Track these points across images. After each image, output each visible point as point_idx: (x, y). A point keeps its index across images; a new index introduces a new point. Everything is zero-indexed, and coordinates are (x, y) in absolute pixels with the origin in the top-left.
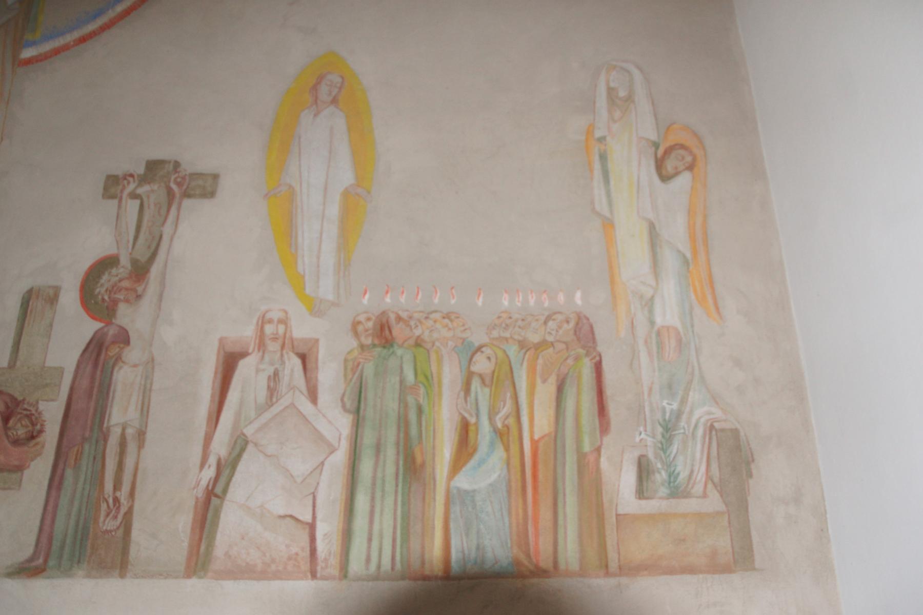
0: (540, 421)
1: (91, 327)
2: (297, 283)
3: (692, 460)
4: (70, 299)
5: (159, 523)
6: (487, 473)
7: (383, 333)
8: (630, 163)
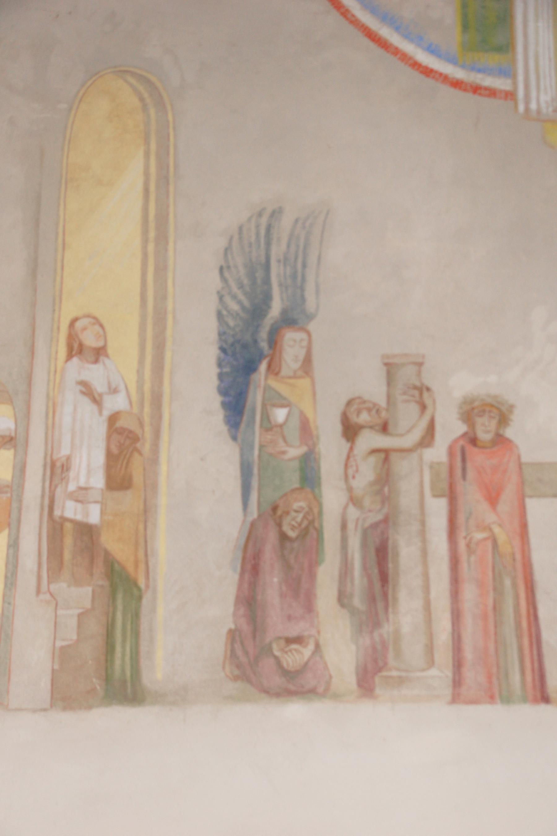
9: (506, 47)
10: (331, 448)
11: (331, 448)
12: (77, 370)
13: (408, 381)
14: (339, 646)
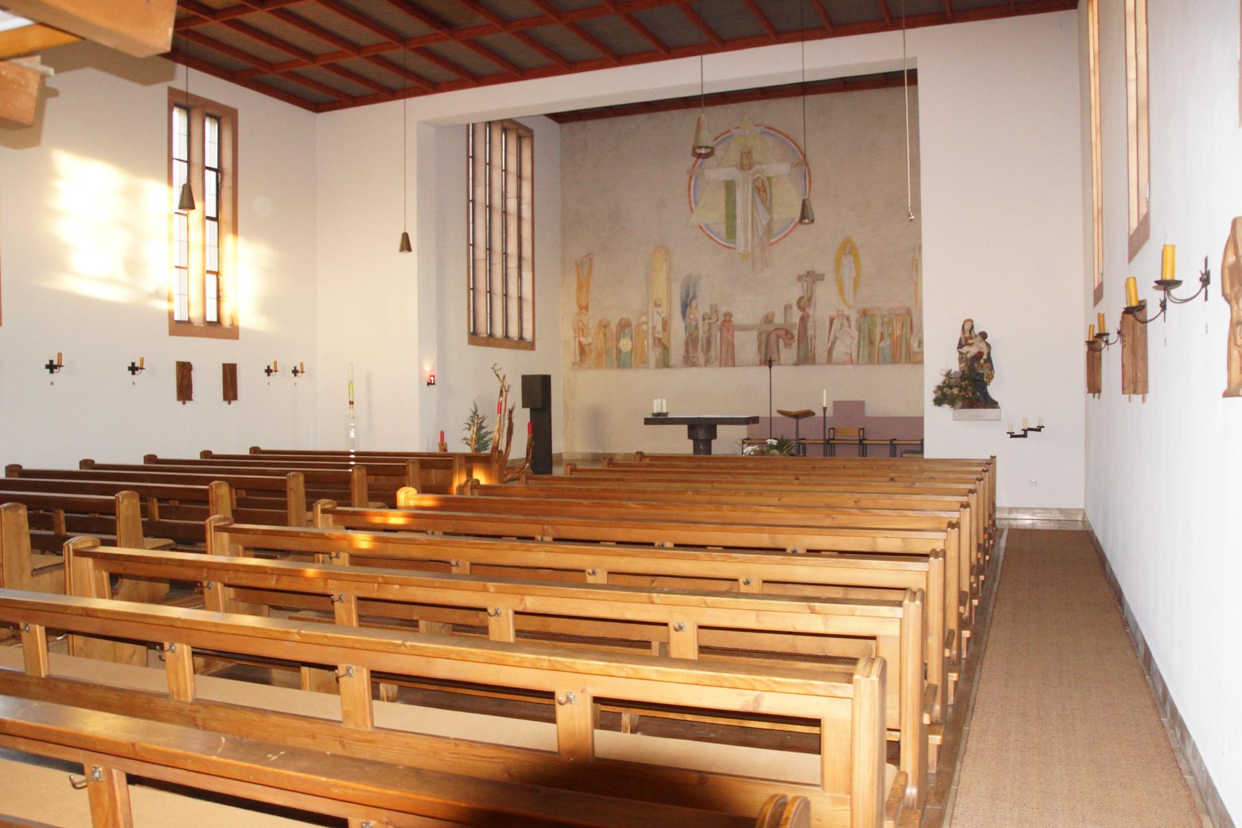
0: (898, 332)
1: (801, 313)
2: (845, 302)
4: (795, 307)
5: (821, 354)
6: (886, 343)
7: (864, 313)
9: (735, 238)
10: (701, 323)
11: (701, 323)
13: (714, 309)
14: (701, 357)
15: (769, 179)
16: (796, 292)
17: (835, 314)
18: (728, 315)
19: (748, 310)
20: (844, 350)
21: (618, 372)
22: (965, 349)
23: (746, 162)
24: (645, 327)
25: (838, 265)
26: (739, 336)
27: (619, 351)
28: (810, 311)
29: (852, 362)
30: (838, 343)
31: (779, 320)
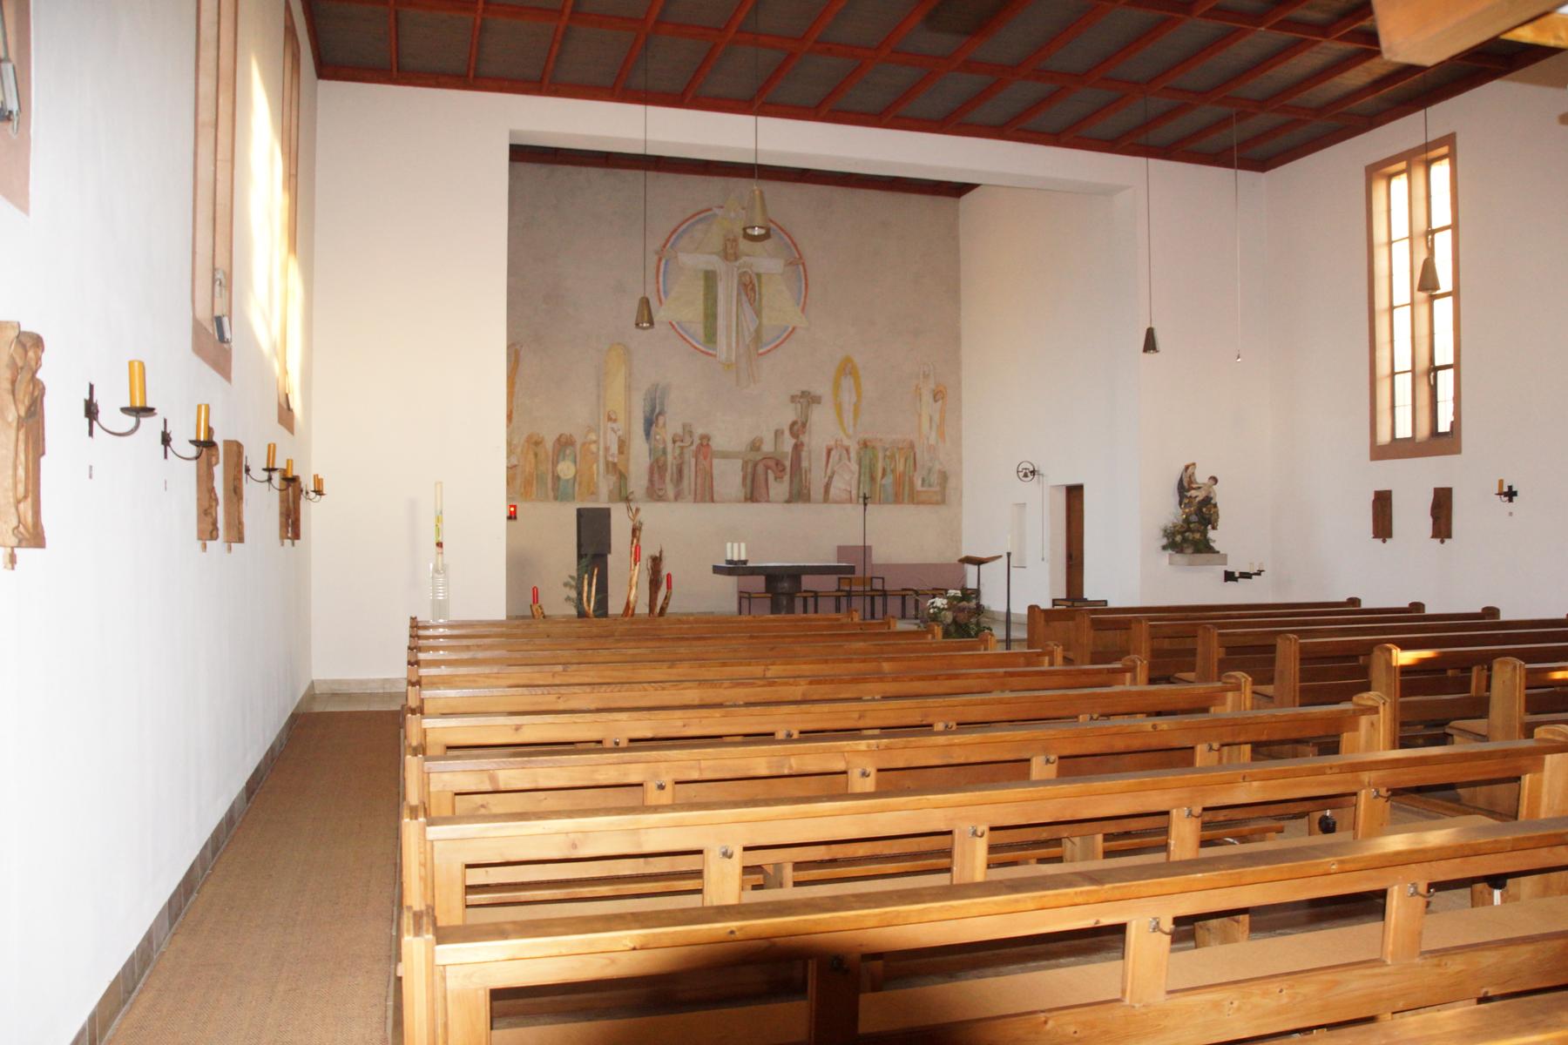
0: (900, 467)
1: (793, 441)
3: (934, 478)
4: (787, 433)
5: (817, 490)
6: (889, 480)
7: (865, 445)
8: (927, 397)
12: (610, 425)
13: (687, 429)
14: (670, 491)
15: (759, 275)
16: (789, 415)
17: (832, 443)
18: (706, 438)
19: (731, 432)
20: (843, 486)
21: (557, 505)
22: (1193, 493)
23: (729, 253)
24: (593, 447)
25: (837, 386)
26: (719, 465)
27: (556, 478)
28: (804, 438)
29: (851, 501)
30: (836, 477)
31: (768, 447)
